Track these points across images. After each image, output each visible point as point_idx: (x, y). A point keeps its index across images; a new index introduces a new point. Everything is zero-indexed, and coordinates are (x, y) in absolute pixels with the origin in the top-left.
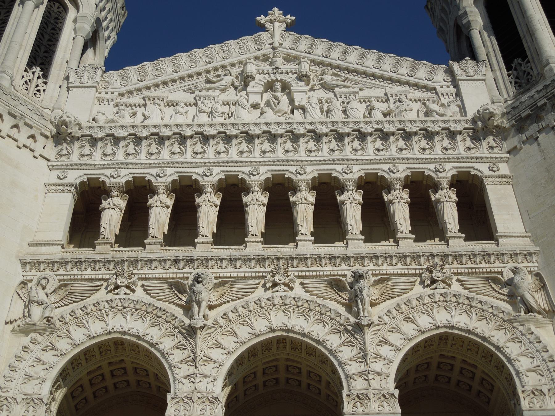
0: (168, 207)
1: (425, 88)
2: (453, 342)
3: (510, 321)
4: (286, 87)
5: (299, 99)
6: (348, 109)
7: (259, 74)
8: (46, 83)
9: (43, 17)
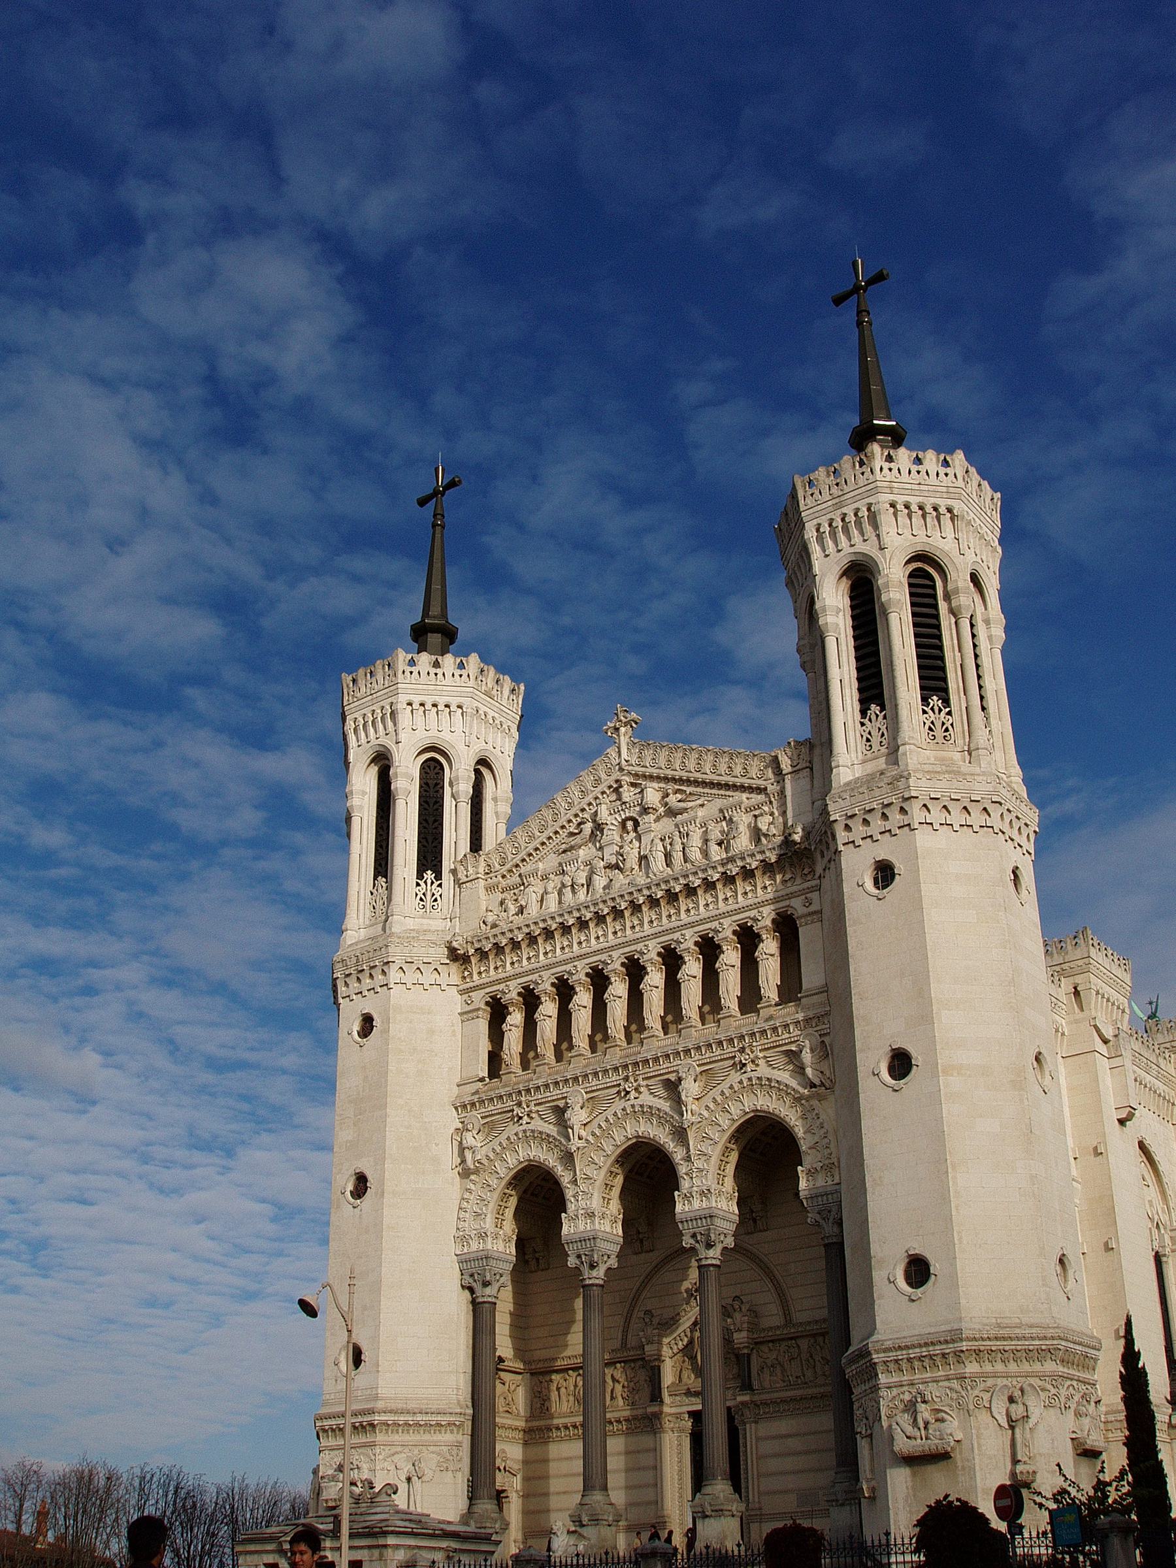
8: (440, 885)
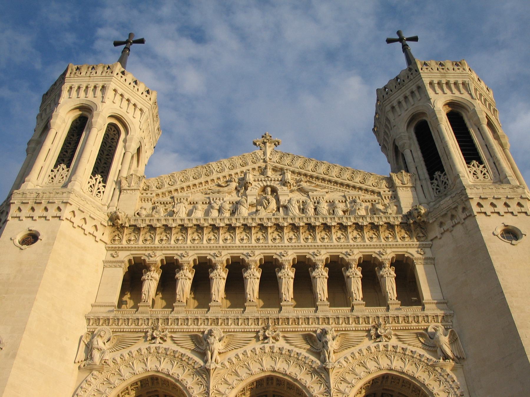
0: (190, 279)
1: (373, 192)
2: (393, 380)
3: (433, 366)
4: (274, 191)
5: (283, 200)
6: (318, 208)
7: (255, 181)
8: (104, 187)
9: (103, 138)
